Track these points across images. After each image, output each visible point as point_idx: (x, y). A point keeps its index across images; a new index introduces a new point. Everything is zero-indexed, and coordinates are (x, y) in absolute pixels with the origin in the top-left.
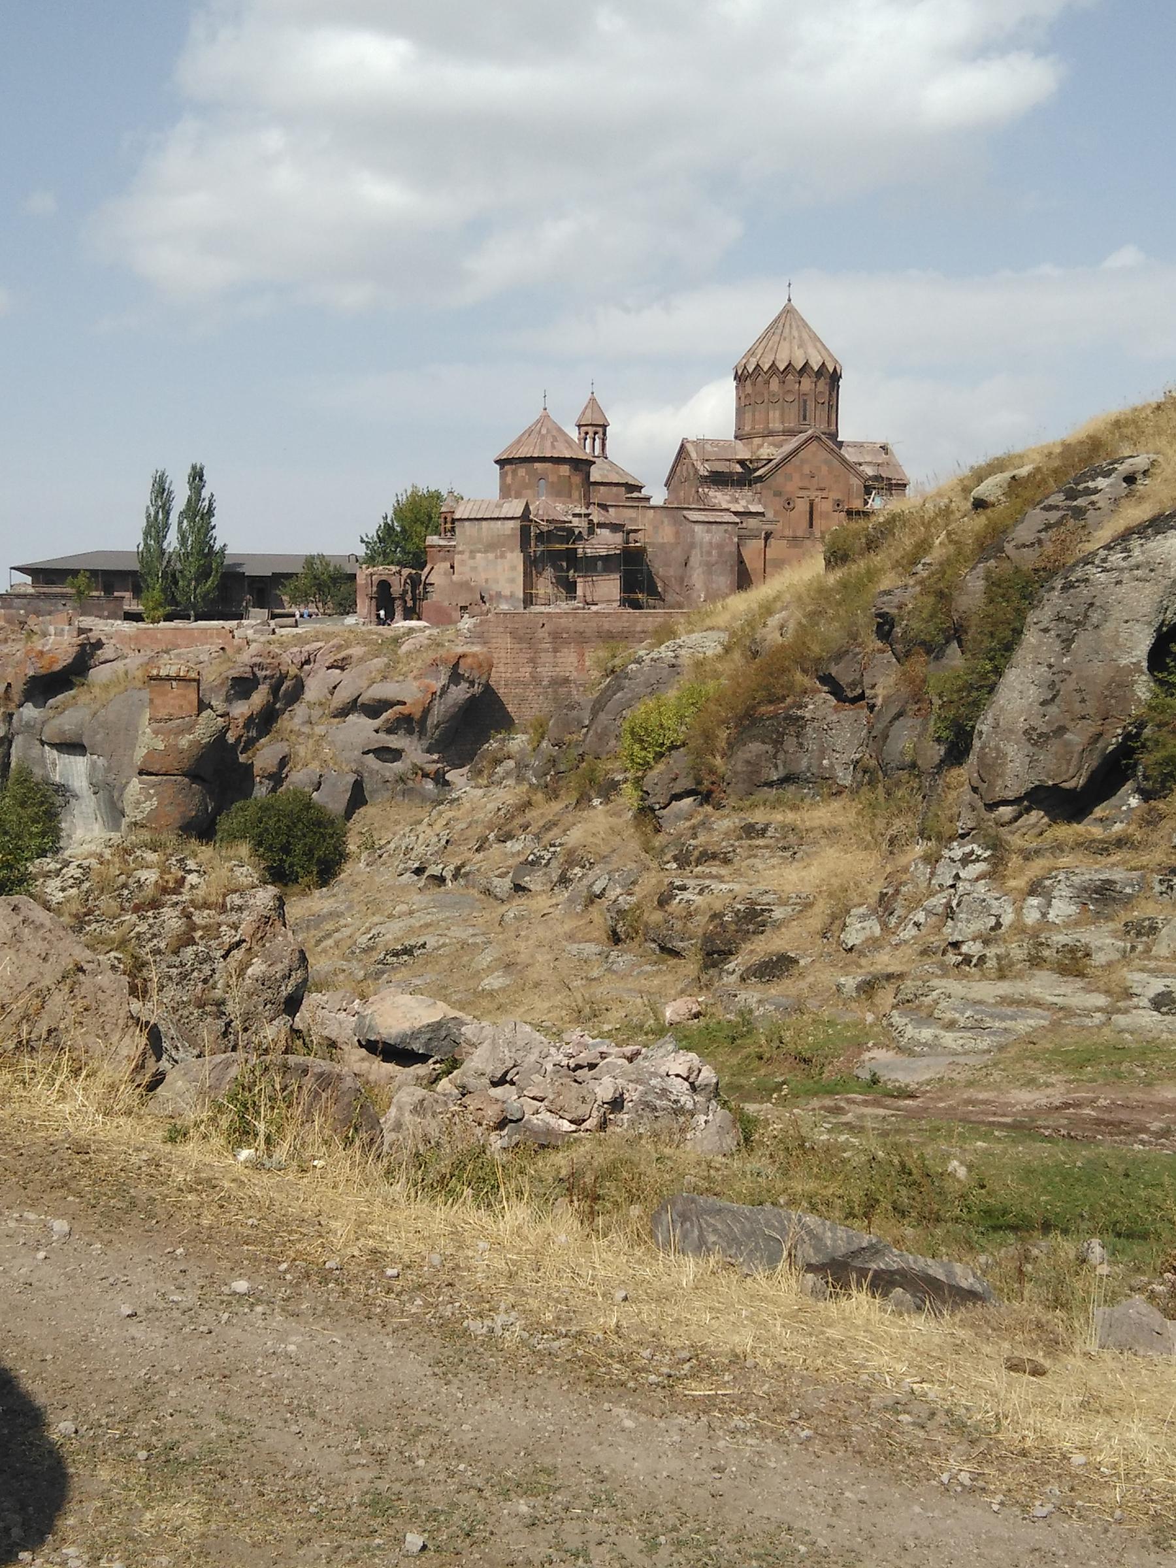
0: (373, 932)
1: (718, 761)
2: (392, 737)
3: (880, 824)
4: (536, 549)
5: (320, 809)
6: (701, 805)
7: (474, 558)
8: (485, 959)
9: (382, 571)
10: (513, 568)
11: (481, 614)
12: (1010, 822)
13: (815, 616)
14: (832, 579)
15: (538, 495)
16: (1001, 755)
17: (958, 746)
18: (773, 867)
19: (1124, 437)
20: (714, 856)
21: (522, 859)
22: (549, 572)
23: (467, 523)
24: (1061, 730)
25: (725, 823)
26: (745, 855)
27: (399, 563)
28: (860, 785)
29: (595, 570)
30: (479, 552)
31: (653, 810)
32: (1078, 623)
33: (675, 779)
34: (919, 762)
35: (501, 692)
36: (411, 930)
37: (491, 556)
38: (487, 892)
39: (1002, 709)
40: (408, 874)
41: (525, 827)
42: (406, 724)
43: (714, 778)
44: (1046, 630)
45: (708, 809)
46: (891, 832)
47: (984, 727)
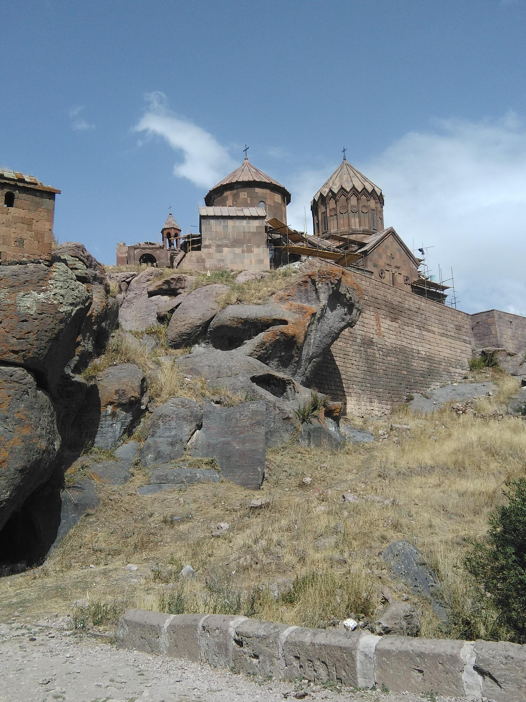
7: (221, 252)
23: (213, 222)
30: (226, 246)
37: (238, 250)
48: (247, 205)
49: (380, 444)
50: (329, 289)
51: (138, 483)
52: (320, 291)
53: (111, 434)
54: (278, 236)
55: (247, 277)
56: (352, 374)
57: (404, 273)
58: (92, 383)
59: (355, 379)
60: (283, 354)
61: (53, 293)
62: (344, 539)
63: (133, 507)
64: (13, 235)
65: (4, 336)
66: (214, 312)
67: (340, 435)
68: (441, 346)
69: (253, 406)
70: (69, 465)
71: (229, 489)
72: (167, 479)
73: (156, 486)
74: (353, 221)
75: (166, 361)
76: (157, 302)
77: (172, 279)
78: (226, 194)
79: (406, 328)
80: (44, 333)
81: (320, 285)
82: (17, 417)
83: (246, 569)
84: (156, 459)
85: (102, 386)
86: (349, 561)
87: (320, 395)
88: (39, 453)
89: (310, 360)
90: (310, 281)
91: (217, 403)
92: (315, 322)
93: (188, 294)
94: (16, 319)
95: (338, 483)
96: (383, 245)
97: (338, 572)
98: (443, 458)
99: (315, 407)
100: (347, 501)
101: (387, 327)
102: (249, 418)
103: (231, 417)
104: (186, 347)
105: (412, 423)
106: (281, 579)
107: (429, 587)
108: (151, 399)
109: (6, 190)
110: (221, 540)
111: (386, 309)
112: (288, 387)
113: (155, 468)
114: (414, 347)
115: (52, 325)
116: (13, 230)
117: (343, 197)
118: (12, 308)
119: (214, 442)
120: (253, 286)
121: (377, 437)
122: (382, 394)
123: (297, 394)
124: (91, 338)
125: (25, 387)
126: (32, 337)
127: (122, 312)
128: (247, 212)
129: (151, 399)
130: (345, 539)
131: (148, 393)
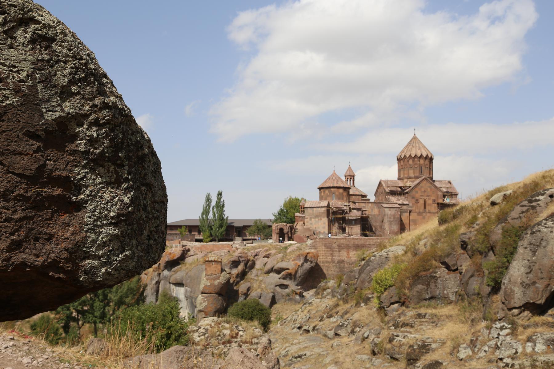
0: (287, 349)
1: (407, 291)
2: (285, 281)
3: (467, 314)
4: (332, 217)
5: (262, 305)
6: (401, 306)
7: (311, 220)
8: (328, 360)
9: (281, 225)
10: (324, 223)
11: (314, 239)
12: (518, 315)
13: (437, 241)
14: (442, 228)
15: (332, 199)
16: (512, 291)
17: (496, 288)
18: (430, 329)
19: (546, 182)
20: (407, 325)
21: (337, 324)
22: (336, 225)
23: (309, 209)
24: (534, 283)
25: (410, 313)
26: (418, 324)
27: (285, 222)
28: (458, 300)
29: (352, 224)
31: (384, 308)
32: (538, 246)
33: (391, 298)
34: (482, 293)
35: (321, 265)
36: (300, 349)
37: (317, 219)
38: (325, 336)
39: (512, 275)
40: (295, 329)
41: (337, 313)
42: (290, 276)
43: (405, 297)
44: (526, 248)
45: (404, 308)
46: (472, 317)
47: (505, 281)
57: (433, 198)
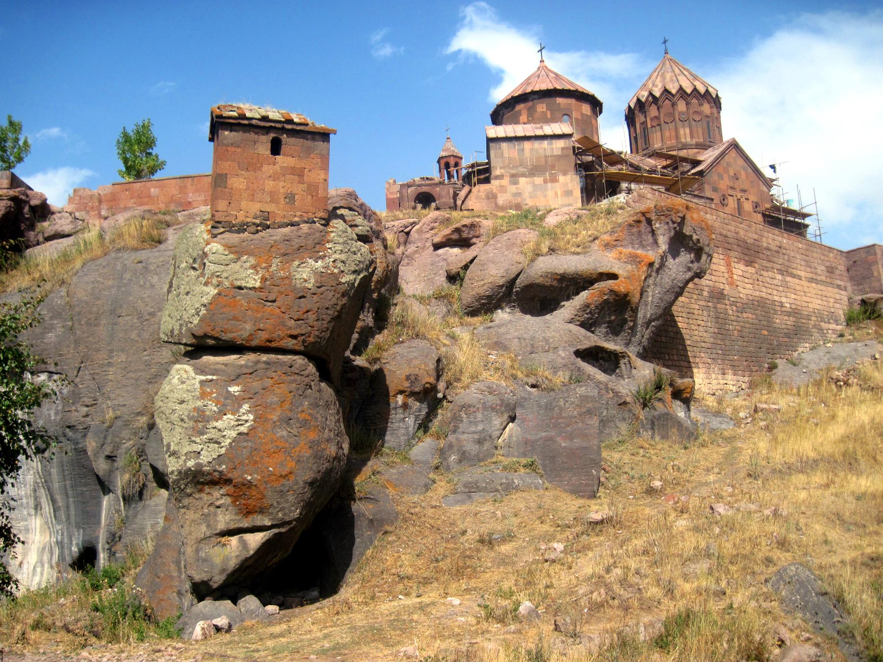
7: (516, 183)
10: (568, 193)
23: (504, 145)
30: (523, 175)
37: (539, 180)
48: (547, 121)
49: (742, 431)
50: (669, 230)
51: (441, 492)
52: (659, 232)
53: (402, 431)
54: (590, 158)
55: (559, 217)
56: (699, 339)
57: (753, 198)
58: (376, 367)
59: (703, 345)
60: (613, 318)
61: (332, 259)
62: (719, 564)
63: (439, 522)
64: (282, 191)
65: (279, 317)
66: (520, 266)
67: (691, 421)
68: (809, 295)
69: (581, 390)
70: (358, 471)
71: (556, 498)
72: (478, 487)
73: (464, 496)
74: (682, 132)
75: (464, 335)
76: (445, 257)
77: (464, 226)
78: (520, 107)
79: (765, 274)
80: (324, 311)
81: (657, 225)
82: (301, 416)
83: (600, 606)
84: (460, 461)
85: (389, 370)
86: (728, 592)
87: (664, 370)
88: (329, 461)
89: (648, 324)
90: (645, 220)
91: (533, 386)
92: (654, 274)
93: (485, 245)
94: (292, 296)
95: (696, 487)
96: (723, 163)
97: (715, 606)
98: (828, 449)
99: (659, 387)
100: (716, 514)
101: (740, 273)
102: (577, 405)
103: (554, 404)
104: (486, 313)
105: (783, 402)
106: (646, 619)
107: (834, 623)
108: (449, 385)
109: (272, 135)
110: (557, 567)
111: (739, 249)
112: (622, 362)
113: (460, 473)
114: (776, 298)
115: (334, 300)
116: (282, 184)
117: (667, 102)
118: (286, 282)
119: (533, 438)
120: (568, 229)
121: (738, 422)
122: (737, 363)
123: (634, 371)
124: (371, 310)
125: (307, 380)
126: (312, 317)
127: (403, 271)
128: (548, 130)
129: (449, 385)
130: (720, 564)
131: (444, 378)
